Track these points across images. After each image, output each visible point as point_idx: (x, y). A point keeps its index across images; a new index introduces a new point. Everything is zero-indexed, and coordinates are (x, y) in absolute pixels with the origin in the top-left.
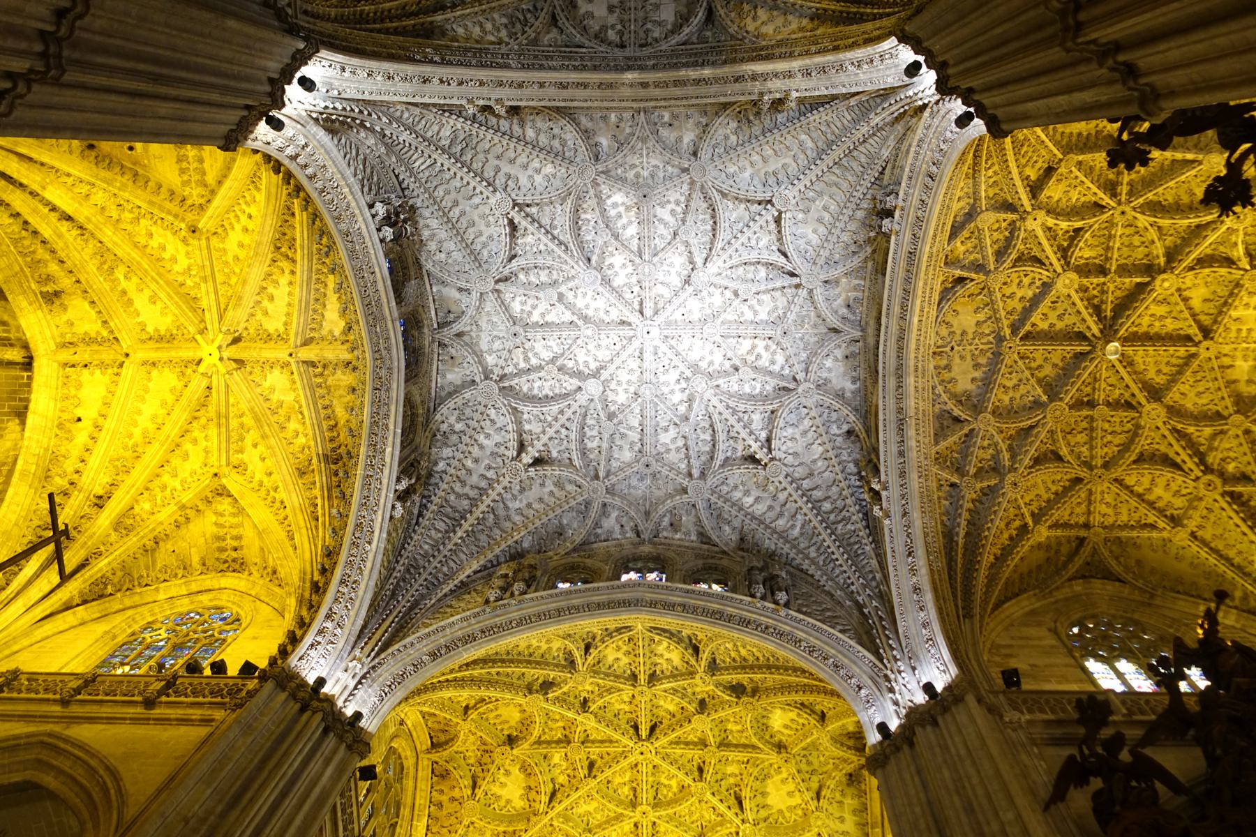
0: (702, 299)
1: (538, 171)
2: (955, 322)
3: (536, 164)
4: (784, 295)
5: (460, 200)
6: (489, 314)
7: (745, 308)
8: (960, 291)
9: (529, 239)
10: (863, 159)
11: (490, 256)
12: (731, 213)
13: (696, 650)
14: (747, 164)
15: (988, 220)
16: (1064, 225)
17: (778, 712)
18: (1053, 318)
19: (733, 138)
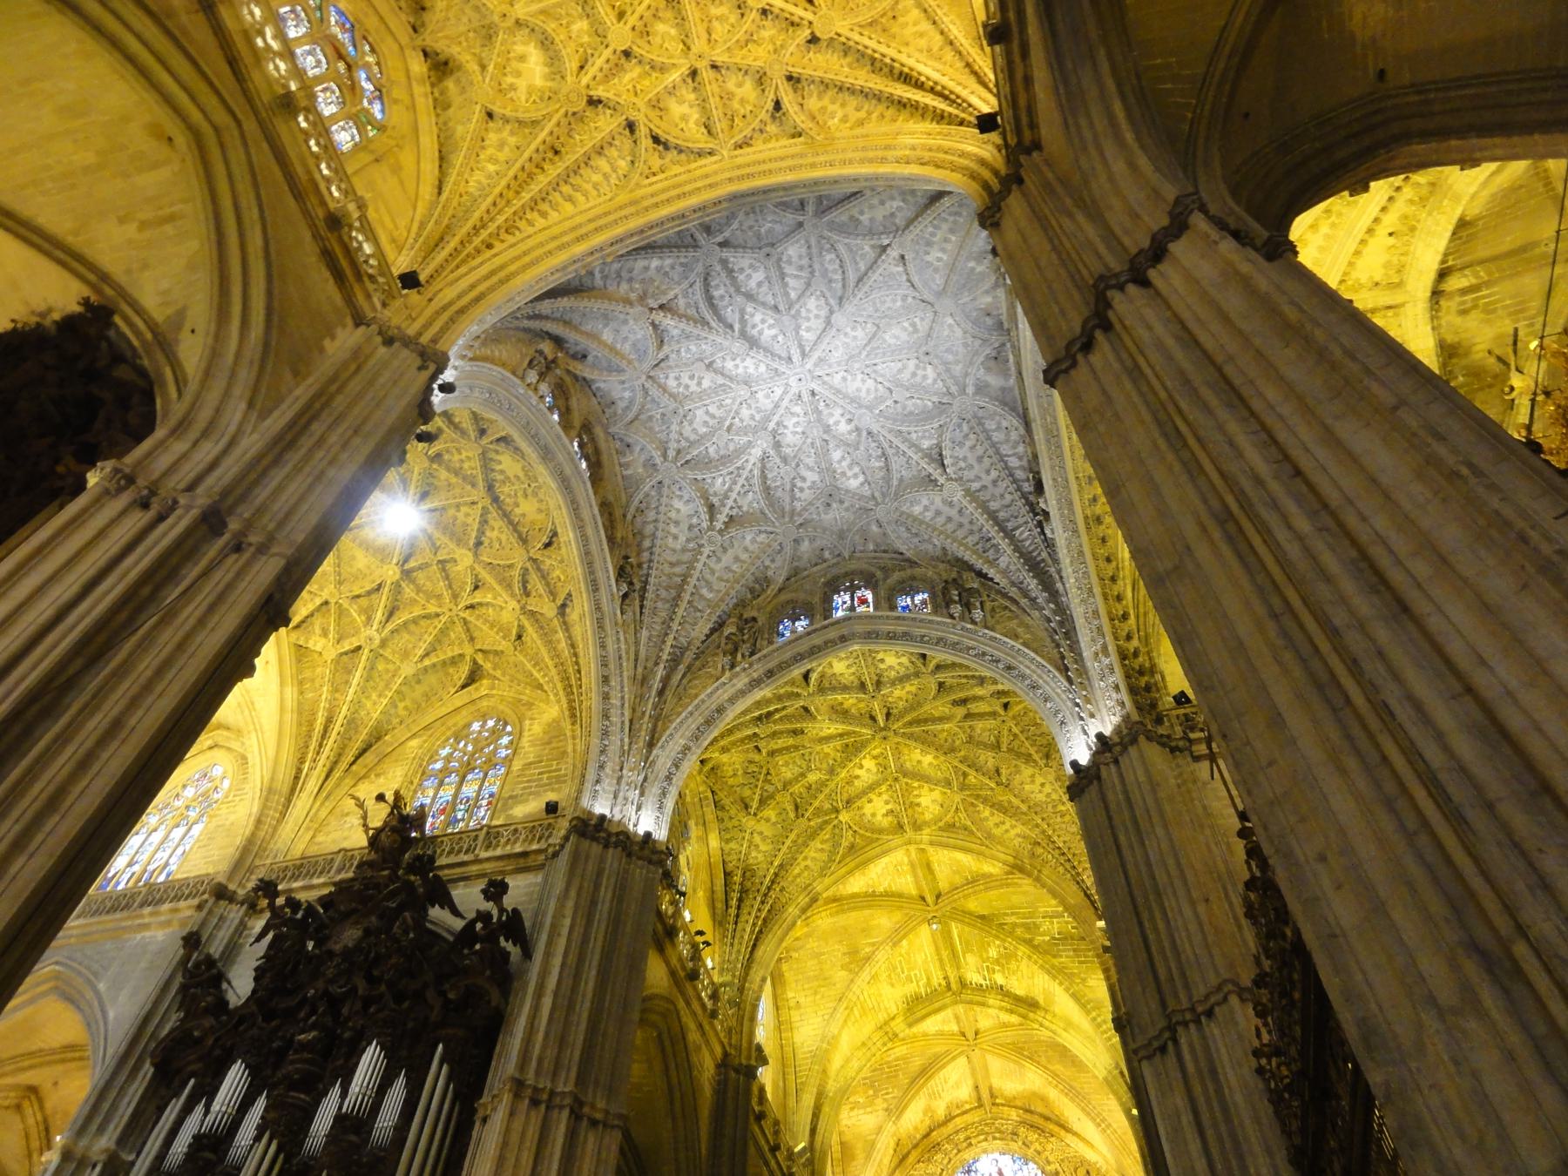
0: (759, 411)
1: (926, 509)
2: (537, 505)
3: (929, 515)
4: (687, 439)
5: (990, 486)
6: (957, 362)
7: (718, 413)
8: (545, 539)
9: (926, 444)
10: (659, 604)
11: (960, 426)
12: (752, 501)
13: (656, 140)
14: (751, 548)
15: (549, 609)
16: (489, 598)
17: (539, 82)
18: (460, 515)
19: (767, 563)
